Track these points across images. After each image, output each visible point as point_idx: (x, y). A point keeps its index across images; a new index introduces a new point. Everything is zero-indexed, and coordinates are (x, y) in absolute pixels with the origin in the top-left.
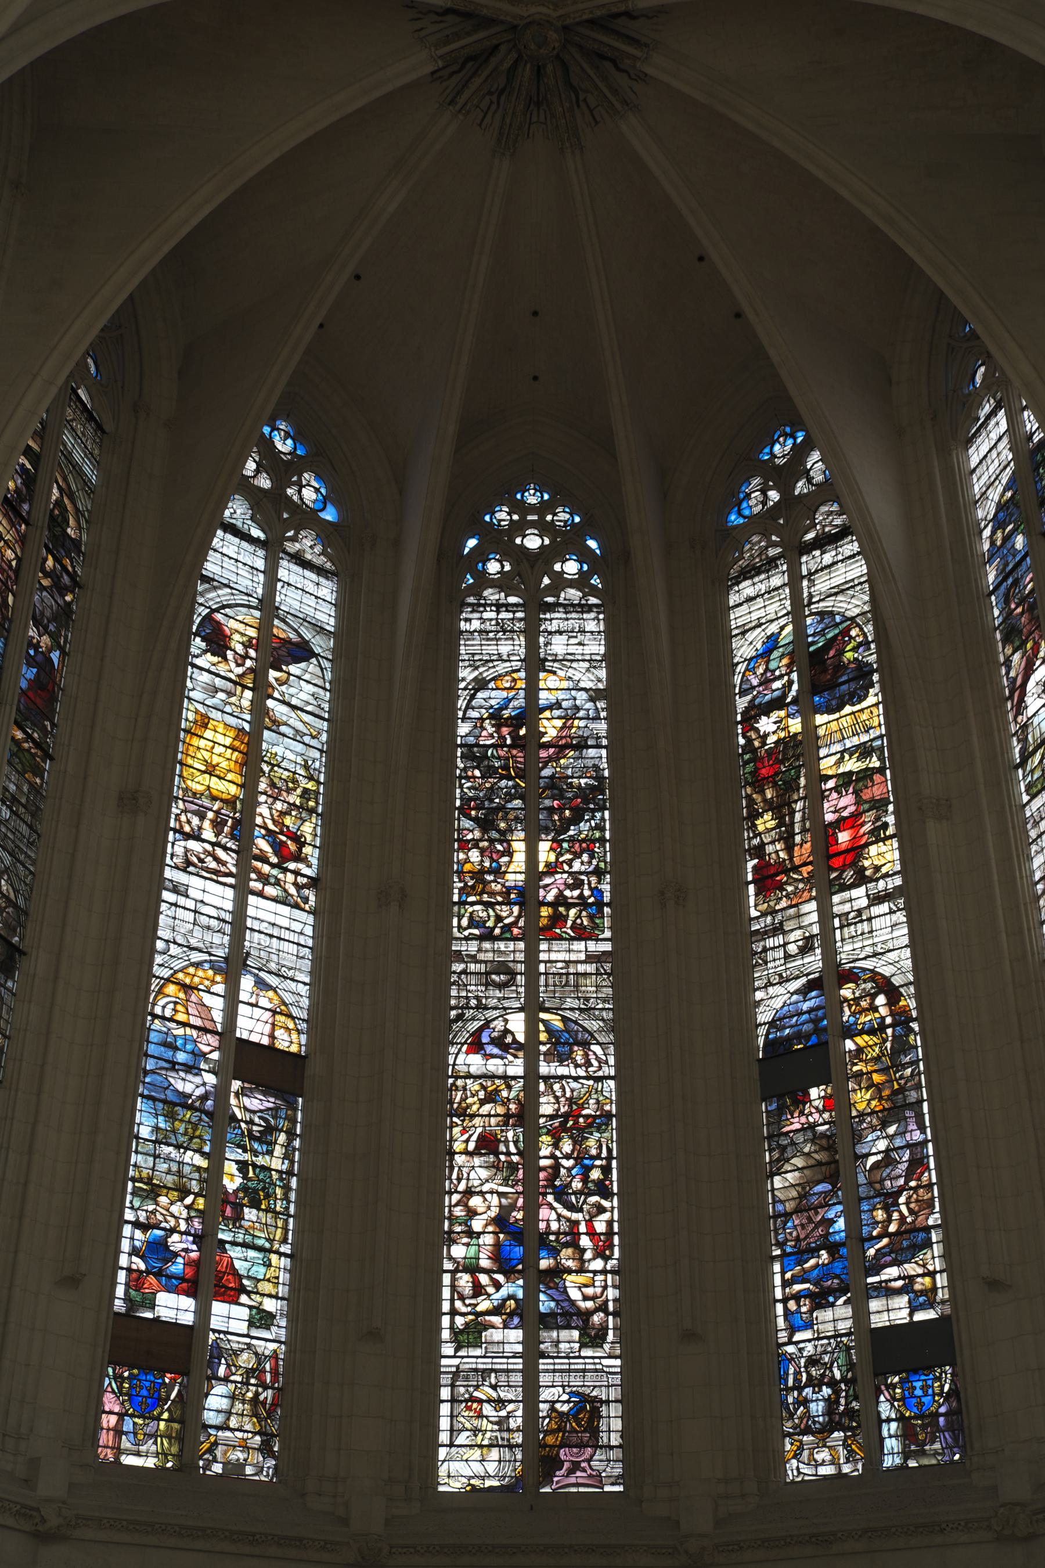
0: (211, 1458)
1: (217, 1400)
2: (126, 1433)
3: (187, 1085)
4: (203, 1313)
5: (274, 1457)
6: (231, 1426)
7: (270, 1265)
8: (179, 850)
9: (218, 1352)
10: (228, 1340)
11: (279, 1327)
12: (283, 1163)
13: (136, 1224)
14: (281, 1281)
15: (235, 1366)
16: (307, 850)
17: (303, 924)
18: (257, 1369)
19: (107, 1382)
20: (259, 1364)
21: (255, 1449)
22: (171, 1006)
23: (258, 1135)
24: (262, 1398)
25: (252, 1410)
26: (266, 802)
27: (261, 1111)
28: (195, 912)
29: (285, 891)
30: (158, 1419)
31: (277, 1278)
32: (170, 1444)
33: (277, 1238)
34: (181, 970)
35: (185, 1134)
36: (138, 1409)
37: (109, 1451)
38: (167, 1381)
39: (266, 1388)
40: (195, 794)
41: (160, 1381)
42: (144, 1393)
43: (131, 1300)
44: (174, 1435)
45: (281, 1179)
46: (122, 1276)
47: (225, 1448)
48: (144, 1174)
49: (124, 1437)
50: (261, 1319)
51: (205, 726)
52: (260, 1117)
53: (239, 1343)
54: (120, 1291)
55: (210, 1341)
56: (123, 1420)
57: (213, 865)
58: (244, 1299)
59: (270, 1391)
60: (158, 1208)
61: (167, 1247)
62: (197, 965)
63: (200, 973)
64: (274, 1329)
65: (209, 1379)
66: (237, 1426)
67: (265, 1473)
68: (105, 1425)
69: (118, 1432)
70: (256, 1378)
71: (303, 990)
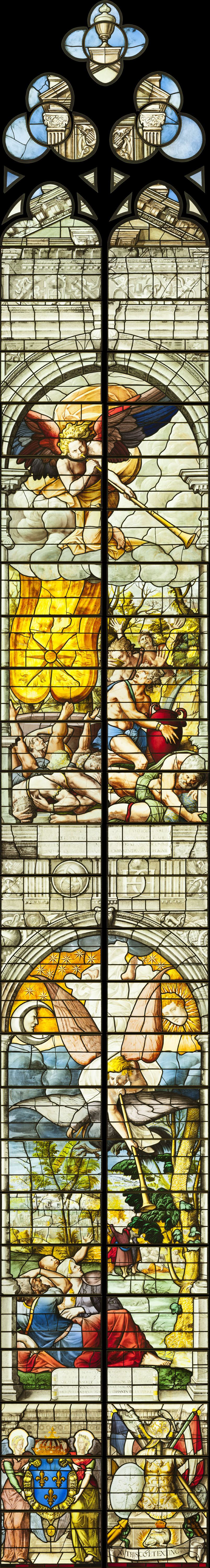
3: (61, 1111)
5: (202, 1536)
6: (146, 1507)
7: (180, 1312)
8: (20, 796)
12: (188, 1180)
13: (18, 1296)
14: (196, 1328)
15: (145, 1438)
16: (190, 729)
17: (192, 841)
18: (173, 1438)
22: (32, 1013)
23: (152, 1151)
24: (182, 1470)
25: (169, 1486)
26: (122, 680)
27: (153, 1120)
28: (50, 875)
29: (163, 803)
31: (192, 1326)
33: (187, 1277)
34: (39, 962)
35: (69, 1171)
39: (186, 1457)
40: (31, 706)
45: (187, 1201)
48: (21, 1235)
51: (36, 595)
52: (152, 1129)
53: (147, 1411)
57: (66, 799)
58: (149, 1359)
59: (193, 1463)
60: (43, 1271)
61: (57, 1315)
62: (59, 949)
63: (64, 958)
64: (191, 1389)
67: (192, 1554)
70: (174, 1448)
71: (200, 938)
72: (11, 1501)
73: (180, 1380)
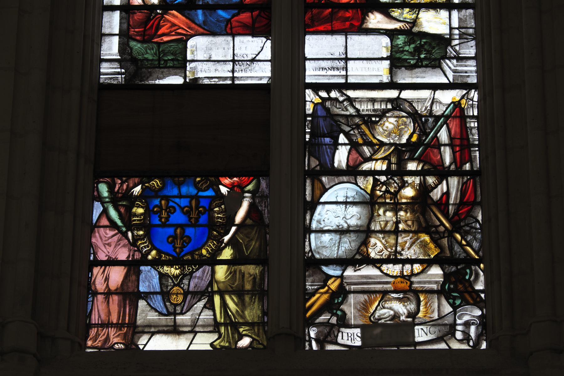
0: (334, 320)
1: (335, 211)
2: (146, 296)
4: (288, 61)
9: (329, 124)
10: (351, 101)
11: (459, 59)
19: (98, 209)
20: (424, 133)
21: (431, 292)
24: (436, 194)
25: (416, 220)
30: (213, 261)
32: (241, 304)
36: (168, 248)
37: (112, 332)
38: (224, 190)
39: (443, 174)
41: (210, 193)
42: (178, 218)
43: (134, 60)
44: (248, 287)
46: (113, 22)
47: (362, 298)
49: (142, 304)
50: (417, 51)
54: (111, 48)
55: (309, 108)
56: (139, 273)
59: (454, 181)
64: (449, 65)
65: (315, 175)
66: (386, 253)
67: (459, 335)
68: (100, 285)
69: (130, 295)
70: (419, 160)
72: (107, 244)
73: (429, 52)
